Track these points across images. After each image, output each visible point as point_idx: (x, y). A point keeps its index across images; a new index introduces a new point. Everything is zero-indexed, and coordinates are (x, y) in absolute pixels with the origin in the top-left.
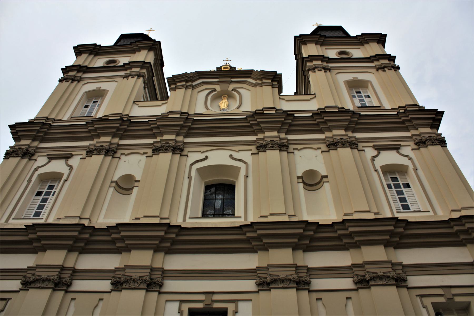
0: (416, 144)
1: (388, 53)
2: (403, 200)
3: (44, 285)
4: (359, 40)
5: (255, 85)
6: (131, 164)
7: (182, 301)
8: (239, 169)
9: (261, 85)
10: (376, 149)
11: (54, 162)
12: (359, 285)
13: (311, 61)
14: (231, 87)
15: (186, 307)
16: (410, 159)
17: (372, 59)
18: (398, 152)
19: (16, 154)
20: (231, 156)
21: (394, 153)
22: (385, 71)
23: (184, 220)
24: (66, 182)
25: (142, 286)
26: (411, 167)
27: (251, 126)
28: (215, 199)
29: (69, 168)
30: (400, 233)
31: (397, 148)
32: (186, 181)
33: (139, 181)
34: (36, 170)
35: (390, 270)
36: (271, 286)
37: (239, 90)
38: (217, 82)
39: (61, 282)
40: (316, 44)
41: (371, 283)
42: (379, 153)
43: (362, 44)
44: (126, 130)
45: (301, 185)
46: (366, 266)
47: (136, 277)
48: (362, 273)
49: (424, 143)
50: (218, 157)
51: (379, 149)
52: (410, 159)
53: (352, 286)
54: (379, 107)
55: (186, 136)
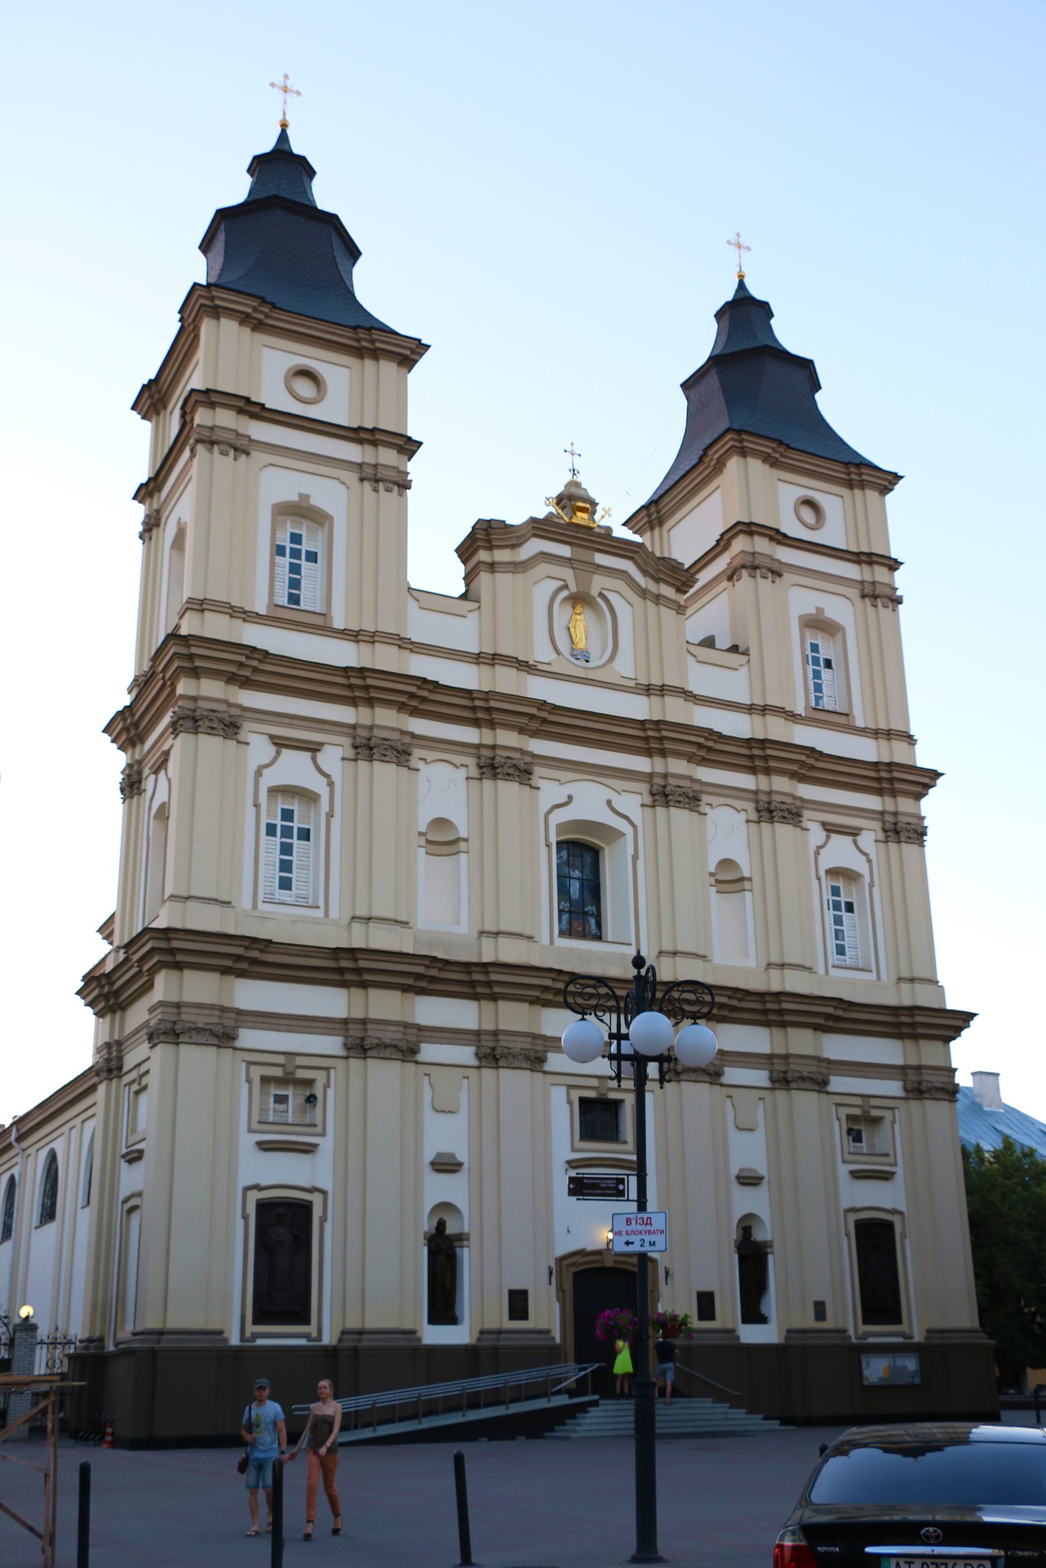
0: (885, 831)
1: (893, 556)
2: (839, 934)
3: (387, 1053)
4: (849, 474)
5: (644, 593)
6: (442, 788)
7: (570, 1087)
8: (622, 834)
9: (658, 599)
10: (827, 830)
11: (288, 755)
12: (777, 1085)
13: (751, 534)
14: (598, 583)
15: (576, 1095)
16: (869, 861)
17: (863, 558)
18: (855, 842)
19: (212, 728)
20: (609, 802)
21: (850, 839)
22: (876, 606)
24: (333, 820)
25: (524, 1065)
27: (646, 739)
28: (570, 878)
29: (325, 780)
30: (838, 1015)
31: (853, 832)
32: (544, 850)
33: (466, 840)
34: (258, 774)
35: (815, 1069)
36: (682, 1077)
37: (609, 595)
38: (570, 559)
39: (405, 1046)
40: (764, 461)
41: (793, 1085)
42: (828, 837)
43: (850, 485)
44: (424, 700)
45: (714, 889)
46: (791, 1060)
47: (518, 1050)
48: (782, 1068)
49: (897, 832)
50: (590, 802)
51: (830, 829)
52: (869, 861)
53: (767, 1084)
54: (847, 715)
55: (535, 734)
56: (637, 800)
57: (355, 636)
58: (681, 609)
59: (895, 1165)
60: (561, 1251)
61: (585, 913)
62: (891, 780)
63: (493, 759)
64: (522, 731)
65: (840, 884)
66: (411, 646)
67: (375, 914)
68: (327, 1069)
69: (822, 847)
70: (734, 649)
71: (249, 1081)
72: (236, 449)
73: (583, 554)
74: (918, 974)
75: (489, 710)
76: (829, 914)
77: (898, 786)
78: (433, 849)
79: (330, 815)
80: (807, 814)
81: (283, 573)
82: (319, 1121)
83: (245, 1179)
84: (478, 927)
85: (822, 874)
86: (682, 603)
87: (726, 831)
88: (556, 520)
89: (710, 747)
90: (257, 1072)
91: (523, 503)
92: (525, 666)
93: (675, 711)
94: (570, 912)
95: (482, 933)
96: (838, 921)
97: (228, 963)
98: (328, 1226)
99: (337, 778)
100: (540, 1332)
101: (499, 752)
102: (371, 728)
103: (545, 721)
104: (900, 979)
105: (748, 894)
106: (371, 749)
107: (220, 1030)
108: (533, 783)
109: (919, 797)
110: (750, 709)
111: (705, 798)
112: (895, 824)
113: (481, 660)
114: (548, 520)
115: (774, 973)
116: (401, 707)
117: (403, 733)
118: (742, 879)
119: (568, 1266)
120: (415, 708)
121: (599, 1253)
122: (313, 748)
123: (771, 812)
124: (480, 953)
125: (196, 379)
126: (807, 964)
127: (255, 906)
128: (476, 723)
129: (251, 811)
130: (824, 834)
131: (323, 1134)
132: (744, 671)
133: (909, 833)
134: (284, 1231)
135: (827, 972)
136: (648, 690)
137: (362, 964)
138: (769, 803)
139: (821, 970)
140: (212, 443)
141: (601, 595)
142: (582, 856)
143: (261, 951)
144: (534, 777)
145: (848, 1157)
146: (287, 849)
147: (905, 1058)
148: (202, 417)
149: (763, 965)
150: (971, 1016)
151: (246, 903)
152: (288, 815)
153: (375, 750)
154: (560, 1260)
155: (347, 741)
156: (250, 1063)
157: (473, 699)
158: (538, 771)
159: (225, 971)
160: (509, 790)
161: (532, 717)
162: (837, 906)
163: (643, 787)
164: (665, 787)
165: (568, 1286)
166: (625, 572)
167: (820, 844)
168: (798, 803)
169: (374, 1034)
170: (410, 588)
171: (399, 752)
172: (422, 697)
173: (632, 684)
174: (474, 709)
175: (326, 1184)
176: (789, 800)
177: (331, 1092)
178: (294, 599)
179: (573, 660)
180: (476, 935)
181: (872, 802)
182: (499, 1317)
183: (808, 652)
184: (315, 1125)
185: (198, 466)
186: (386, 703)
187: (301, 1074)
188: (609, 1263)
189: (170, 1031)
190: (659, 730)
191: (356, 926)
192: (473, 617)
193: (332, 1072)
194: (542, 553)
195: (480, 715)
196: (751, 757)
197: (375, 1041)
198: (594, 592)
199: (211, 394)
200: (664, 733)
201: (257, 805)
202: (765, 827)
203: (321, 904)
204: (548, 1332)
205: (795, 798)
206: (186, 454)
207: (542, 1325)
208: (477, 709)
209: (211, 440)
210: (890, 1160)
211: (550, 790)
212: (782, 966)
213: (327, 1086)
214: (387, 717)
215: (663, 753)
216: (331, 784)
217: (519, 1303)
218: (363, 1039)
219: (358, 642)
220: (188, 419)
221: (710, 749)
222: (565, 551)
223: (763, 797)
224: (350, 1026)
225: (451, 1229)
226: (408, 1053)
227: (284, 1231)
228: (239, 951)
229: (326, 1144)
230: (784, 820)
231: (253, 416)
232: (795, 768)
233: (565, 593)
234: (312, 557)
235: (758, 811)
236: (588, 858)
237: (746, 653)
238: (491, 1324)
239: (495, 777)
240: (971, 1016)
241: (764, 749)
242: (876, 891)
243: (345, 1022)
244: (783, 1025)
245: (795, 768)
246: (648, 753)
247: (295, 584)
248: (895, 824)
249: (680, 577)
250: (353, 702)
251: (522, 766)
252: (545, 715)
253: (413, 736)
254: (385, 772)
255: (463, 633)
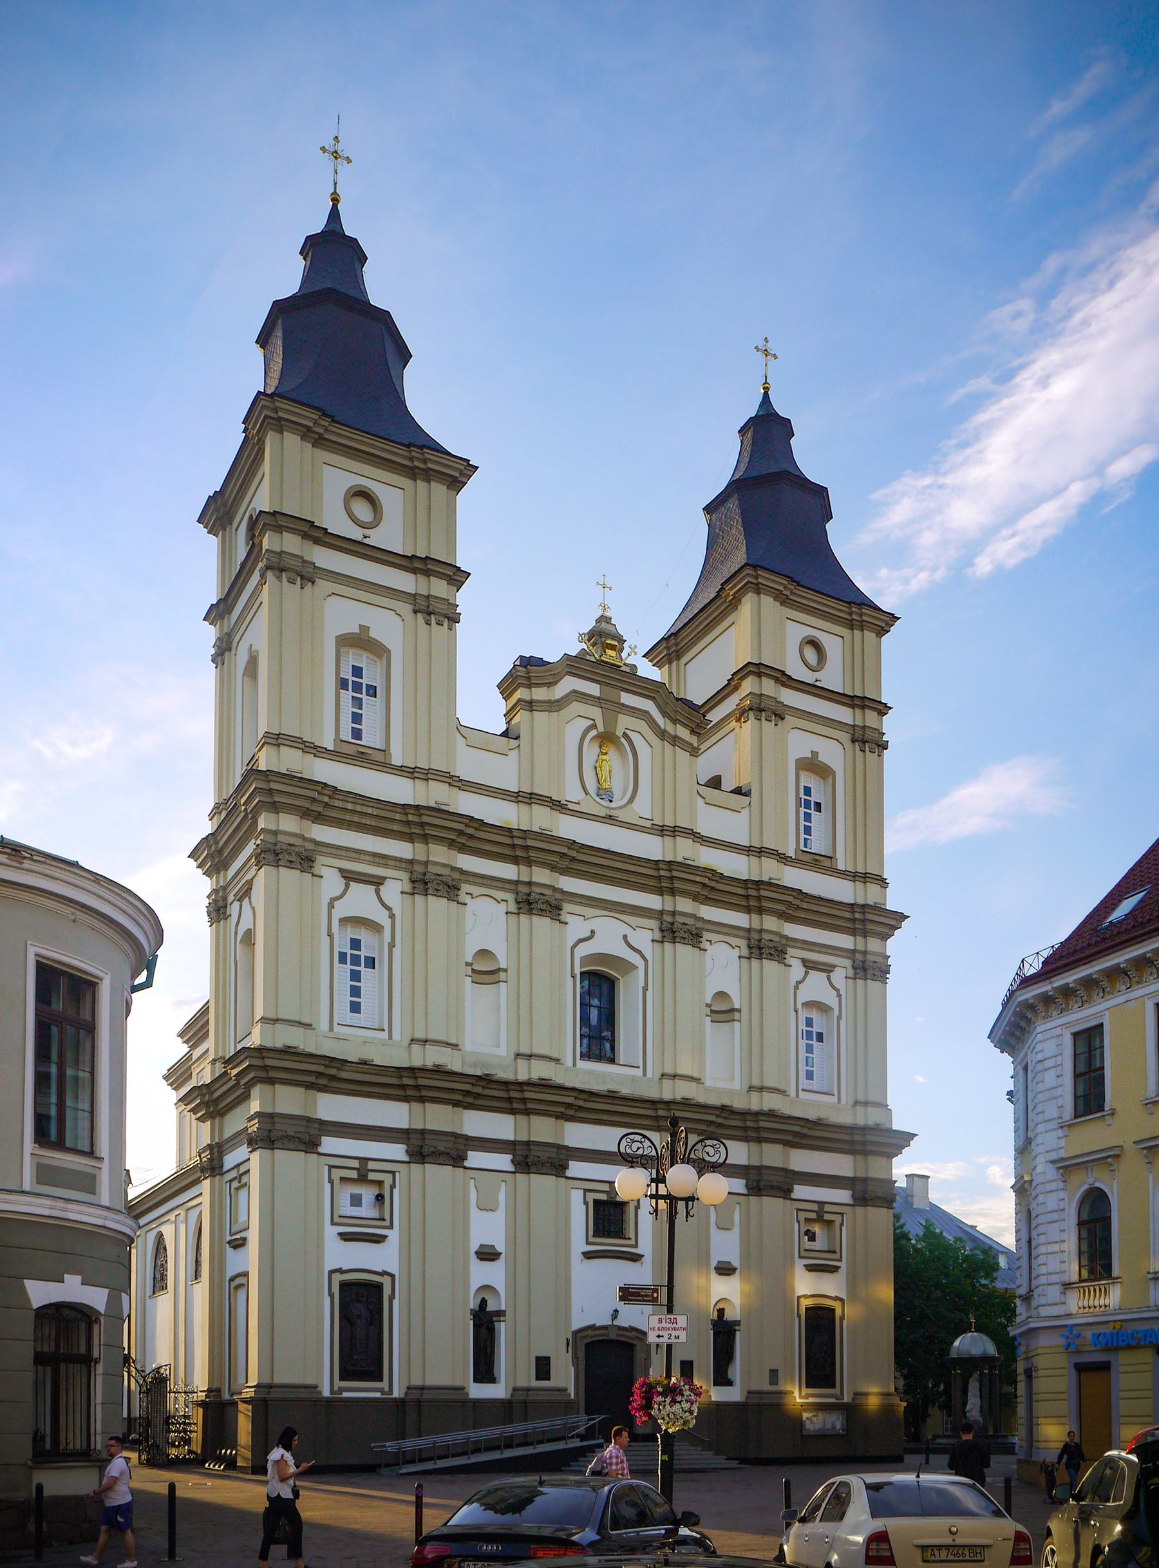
5: (662, 734)
6: (486, 921)
9: (675, 740)
16: (839, 996)
18: (829, 978)
20: (625, 937)
23: (574, 1064)
26: (836, 1013)
27: (659, 878)
31: (828, 969)
32: (570, 980)
33: (506, 970)
38: (599, 698)
42: (806, 973)
49: (865, 970)
50: (609, 936)
51: (809, 965)
52: (839, 996)
55: (565, 872)
56: (649, 935)
57: (411, 772)
58: (694, 752)
59: (840, 1260)
60: (575, 1326)
61: (603, 1038)
62: (864, 921)
63: (529, 895)
64: (553, 868)
65: (814, 1015)
66: (459, 784)
67: (430, 1037)
68: (393, 1173)
69: (801, 982)
70: (738, 791)
71: (331, 1181)
72: (302, 577)
73: (611, 693)
74: (871, 1098)
75: (526, 848)
76: (803, 1043)
77: (869, 926)
78: (478, 978)
79: (392, 945)
80: (791, 951)
81: (347, 709)
82: (387, 1217)
83: (330, 1263)
84: (514, 1050)
85: (799, 1006)
86: (696, 745)
87: (721, 966)
88: (588, 658)
89: (713, 887)
90: (337, 1174)
91: (559, 641)
92: (558, 806)
93: (684, 850)
94: (589, 1037)
95: (518, 1055)
96: (810, 1049)
97: (312, 1079)
98: (396, 1302)
99: (397, 911)
100: (558, 1390)
101: (534, 889)
102: (426, 863)
103: (573, 859)
104: (856, 1103)
105: (737, 1024)
106: (426, 883)
107: (306, 1138)
108: (562, 918)
109: (885, 937)
110: (748, 851)
111: (706, 935)
112: (864, 962)
113: (520, 799)
114: (580, 658)
115: (755, 1095)
116: (452, 844)
117: (453, 868)
118: (733, 1010)
119: (582, 1338)
120: (464, 844)
121: (605, 1328)
122: (377, 882)
123: (761, 949)
124: (516, 1074)
125: (262, 499)
126: (782, 1087)
127: (331, 1029)
128: (515, 860)
129: (326, 940)
130: (804, 969)
131: (391, 1227)
132: (745, 812)
133: (872, 970)
134: (361, 1302)
135: (797, 1096)
136: (662, 831)
137: (421, 1082)
138: (760, 941)
139: (793, 1094)
140: (282, 570)
141: (625, 735)
142: (600, 986)
143: (338, 1069)
144: (563, 913)
145: (803, 1254)
146: (355, 976)
147: (855, 1170)
148: (268, 541)
149: (746, 1088)
150: (912, 1136)
151: (324, 1025)
152: (356, 944)
153: (429, 885)
154: (575, 1333)
155: (405, 876)
156: (331, 1167)
157: (512, 837)
158: (567, 907)
159: (309, 1086)
160: (542, 923)
161: (563, 855)
162: (809, 1035)
163: (654, 924)
164: (672, 924)
165: (581, 1354)
166: (648, 712)
167: (799, 979)
168: (784, 941)
169: (431, 1143)
170: (460, 727)
171: (448, 886)
172: (470, 835)
173: (648, 824)
174: (513, 846)
175: (394, 1270)
176: (776, 938)
177: (396, 1192)
178: (357, 734)
179: (597, 799)
180: (512, 1057)
181: (844, 941)
182: (527, 1378)
183: (802, 795)
184: (383, 1220)
185: (268, 594)
186: (438, 841)
187: (372, 1176)
188: (613, 1336)
189: (274, 1134)
190: (670, 871)
191: (415, 1047)
192: (514, 754)
193: (397, 1175)
194: (574, 691)
195: (519, 853)
196: (747, 897)
197: (432, 1149)
198: (619, 733)
199: (278, 516)
200: (675, 873)
201: (330, 935)
202: (755, 963)
203: (386, 1027)
204: (565, 1390)
205: (782, 936)
206: (256, 577)
207: (561, 1385)
208: (517, 846)
209: (280, 566)
210: (837, 1256)
211: (576, 924)
212: (761, 1089)
213: (393, 1186)
214: (439, 854)
215: (673, 892)
216: (392, 916)
217: (543, 1367)
218: (421, 1147)
219: (414, 778)
220: (257, 541)
221: (713, 888)
222: (594, 689)
223: (755, 936)
224: (411, 1136)
225: (490, 1307)
226: (457, 1160)
227: (361, 1302)
228: (321, 1069)
229: (393, 1235)
230: (771, 957)
231: (317, 541)
232: (782, 908)
233: (593, 733)
234: (372, 691)
235: (750, 947)
236: (605, 987)
237: (747, 794)
238: (522, 1383)
239: (530, 912)
240: (912, 1136)
241: (758, 890)
242: (843, 1023)
243: (407, 1131)
244: (759, 1140)
245: (782, 908)
246: (660, 891)
247: (357, 718)
248: (864, 962)
249: (692, 720)
250: (410, 838)
251: (554, 903)
252: (574, 854)
253: (461, 871)
254: (438, 905)
255: (504, 772)
